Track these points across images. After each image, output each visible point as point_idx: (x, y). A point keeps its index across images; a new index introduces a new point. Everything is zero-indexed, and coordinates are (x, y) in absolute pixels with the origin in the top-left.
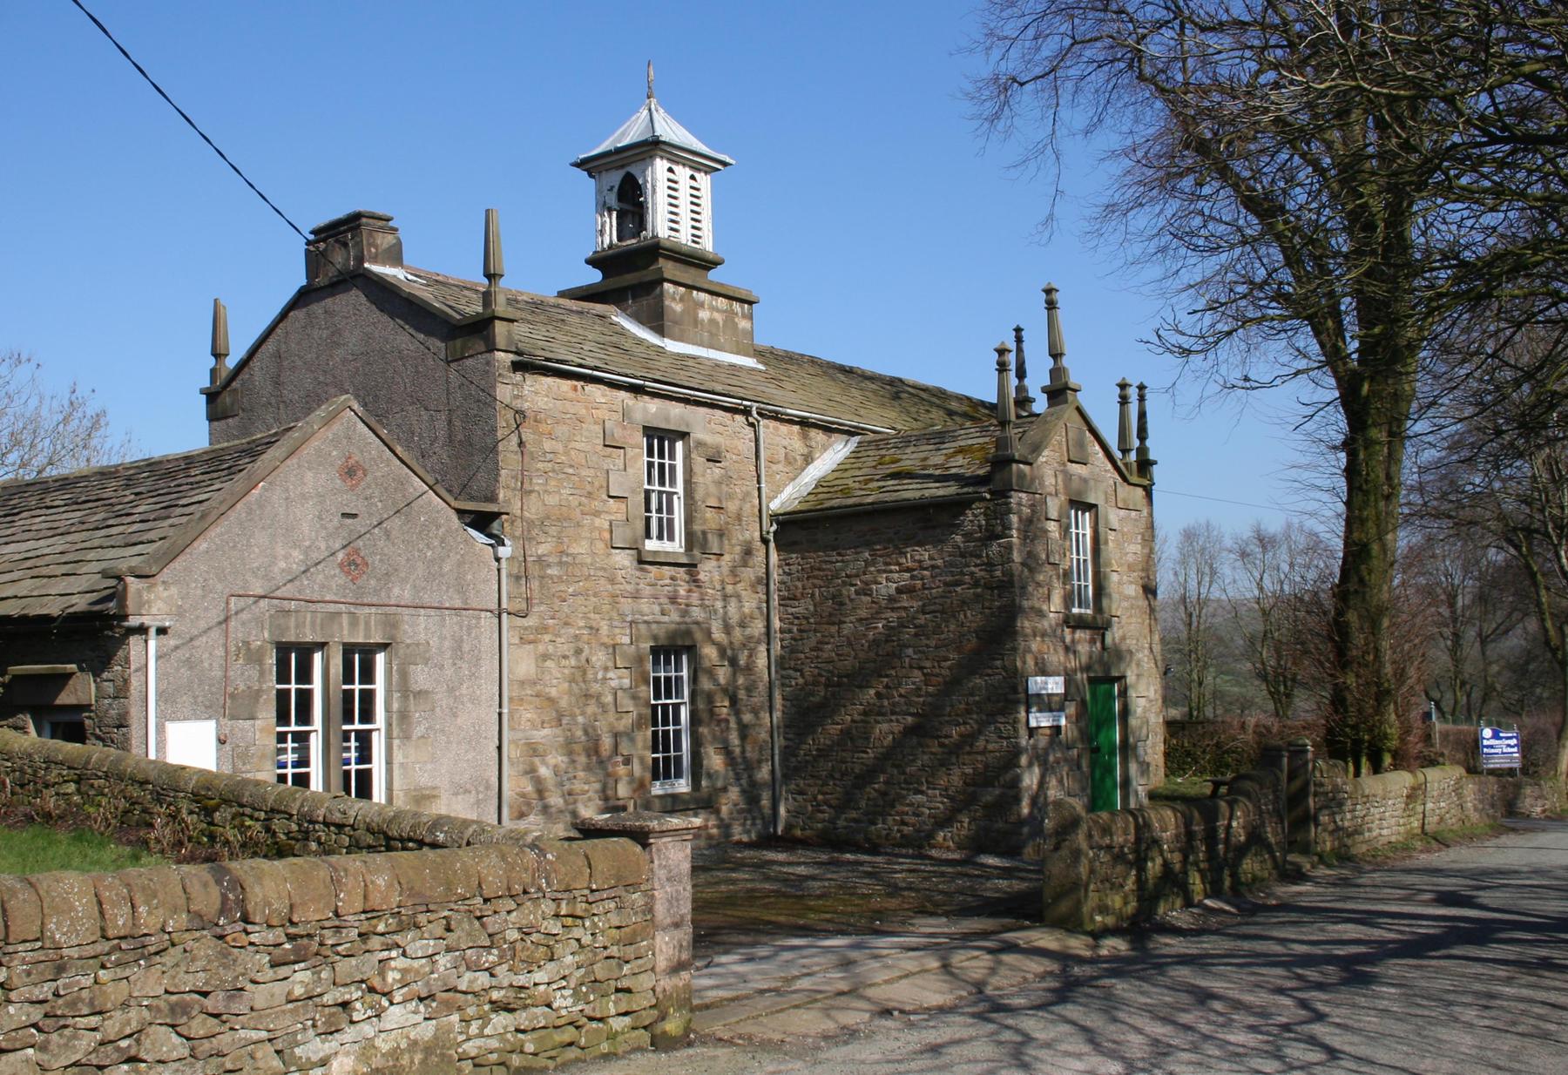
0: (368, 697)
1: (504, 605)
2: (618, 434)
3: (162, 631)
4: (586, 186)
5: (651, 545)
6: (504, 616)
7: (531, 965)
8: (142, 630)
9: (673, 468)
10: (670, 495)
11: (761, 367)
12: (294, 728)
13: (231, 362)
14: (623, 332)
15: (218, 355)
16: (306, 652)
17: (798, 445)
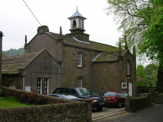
0: (40, 84)
1: (62, 73)
2: (75, 53)
3: (25, 76)
4: (69, 21)
5: (78, 66)
6: (62, 75)
7: (78, 114)
8: (23, 76)
9: (81, 57)
10: (80, 60)
11: (90, 44)
12: (39, 87)
13: (28, 43)
14: (74, 40)
15: (26, 41)
16: (40, 79)
17: (95, 53)
